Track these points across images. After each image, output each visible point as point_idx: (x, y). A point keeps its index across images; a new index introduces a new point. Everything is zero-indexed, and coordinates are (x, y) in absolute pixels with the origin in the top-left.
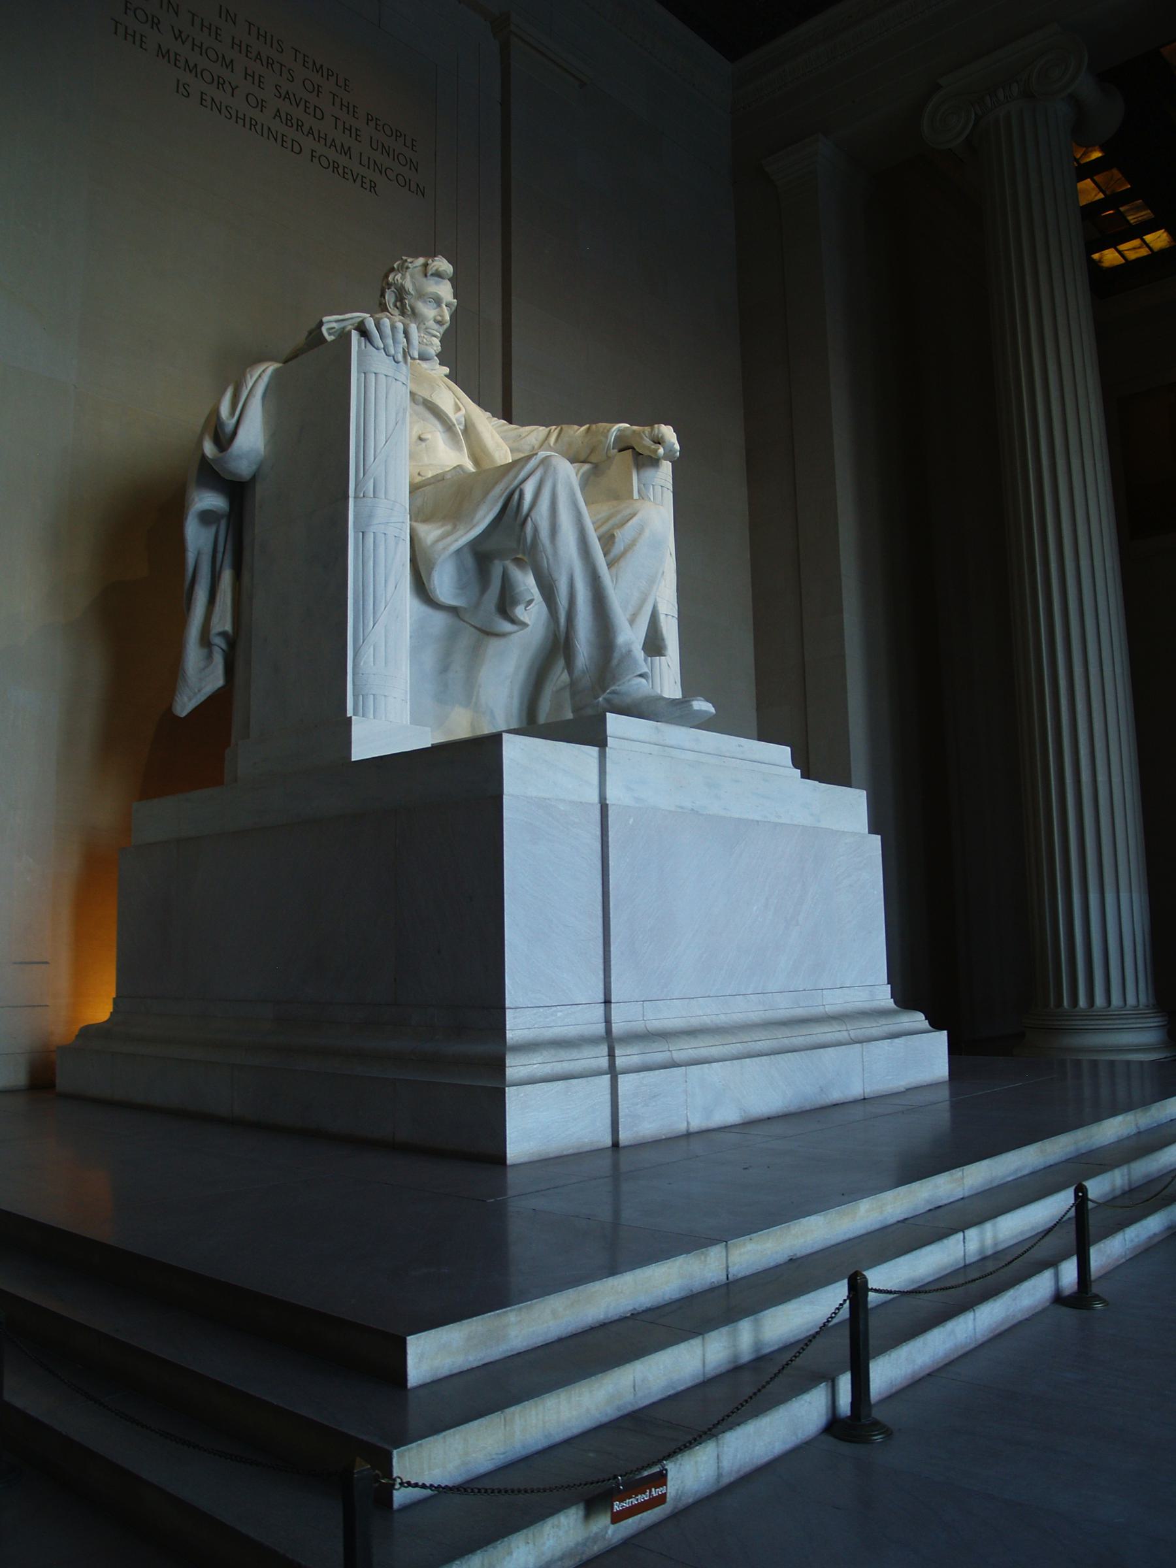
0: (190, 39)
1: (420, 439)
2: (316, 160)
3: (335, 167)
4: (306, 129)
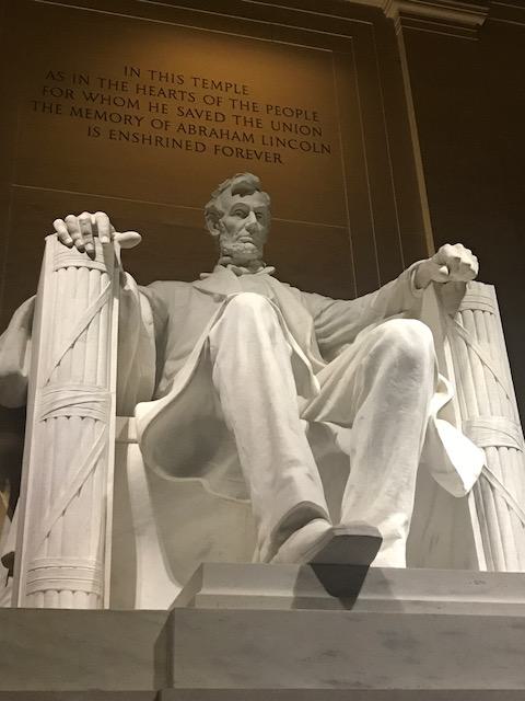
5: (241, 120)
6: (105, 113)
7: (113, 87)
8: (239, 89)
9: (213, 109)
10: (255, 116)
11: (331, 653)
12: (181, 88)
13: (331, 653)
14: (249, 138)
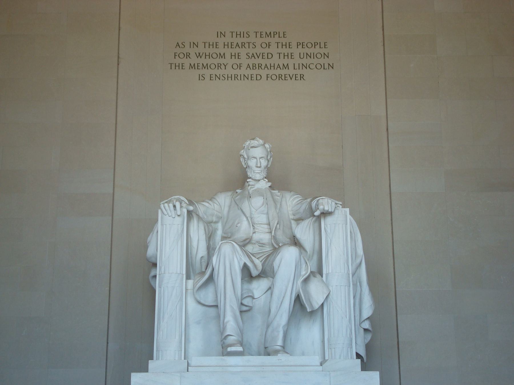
0: (204, 54)
2: (269, 79)
3: (280, 77)
4: (263, 67)
7: (211, 47)
8: (282, 35)
9: (267, 51)
10: (289, 51)
12: (248, 40)
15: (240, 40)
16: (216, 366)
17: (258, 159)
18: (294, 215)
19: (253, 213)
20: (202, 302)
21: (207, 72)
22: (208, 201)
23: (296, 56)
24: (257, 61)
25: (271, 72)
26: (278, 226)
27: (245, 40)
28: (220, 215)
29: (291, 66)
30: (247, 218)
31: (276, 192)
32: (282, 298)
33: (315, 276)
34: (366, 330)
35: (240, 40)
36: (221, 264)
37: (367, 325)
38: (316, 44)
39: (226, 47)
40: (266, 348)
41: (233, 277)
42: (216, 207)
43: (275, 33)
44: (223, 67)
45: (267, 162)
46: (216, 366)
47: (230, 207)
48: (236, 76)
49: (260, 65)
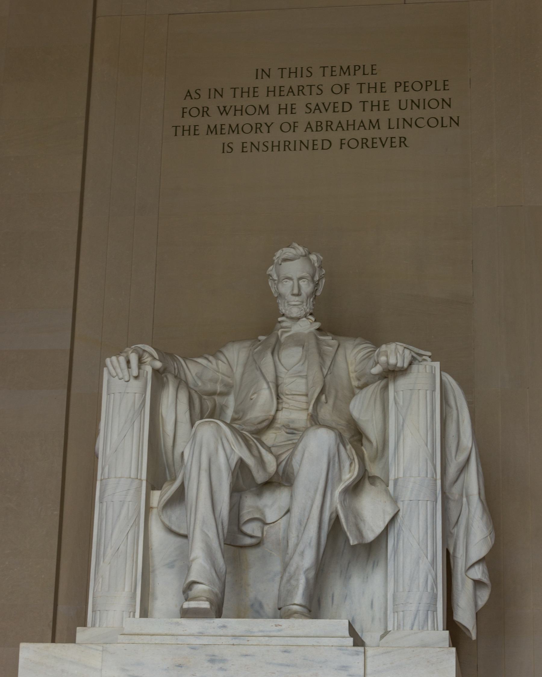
0: (233, 108)
1: (252, 399)
2: (345, 146)
3: (364, 143)
4: (334, 127)
5: (368, 106)
6: (237, 125)
8: (368, 70)
9: (341, 98)
11: (180, 666)
12: (310, 81)
13: (180, 666)
14: (375, 125)
15: (294, 82)
16: (166, 635)
17: (295, 281)
18: (359, 380)
19: (283, 375)
20: (174, 528)
21: (236, 139)
22: (207, 356)
23: (393, 105)
24: (324, 117)
25: (348, 135)
26: (323, 397)
27: (305, 81)
28: (230, 380)
29: (384, 124)
30: (268, 383)
31: (328, 338)
32: (306, 520)
33: (373, 484)
34: (477, 583)
35: (294, 82)
36: (194, 459)
37: (478, 573)
38: (429, 83)
39: (271, 94)
40: (280, 609)
41: (214, 483)
42: (223, 367)
43: (357, 68)
44: (264, 128)
45: (312, 285)
46: (166, 635)
47: (245, 365)
48: (287, 143)
49: (329, 123)
